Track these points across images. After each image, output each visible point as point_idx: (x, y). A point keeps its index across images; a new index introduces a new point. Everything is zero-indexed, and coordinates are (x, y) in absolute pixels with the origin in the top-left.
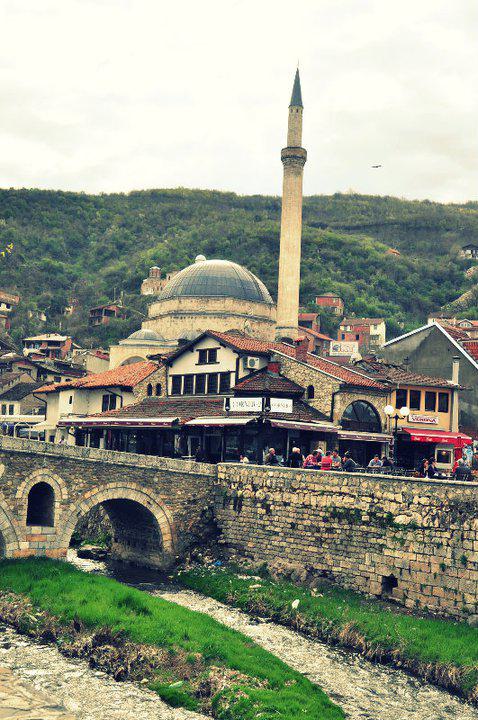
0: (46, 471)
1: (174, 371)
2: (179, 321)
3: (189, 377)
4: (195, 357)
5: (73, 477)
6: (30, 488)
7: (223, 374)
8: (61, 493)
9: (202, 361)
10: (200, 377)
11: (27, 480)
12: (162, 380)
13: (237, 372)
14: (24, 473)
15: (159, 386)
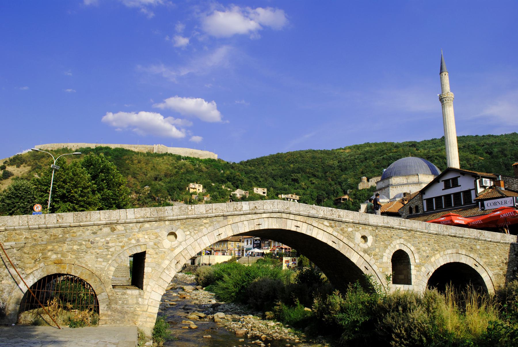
0: (402, 241)
1: (427, 196)
2: (394, 189)
3: (438, 199)
4: (442, 185)
5: (421, 245)
6: (392, 254)
7: (465, 192)
8: (414, 260)
9: (447, 187)
10: (447, 197)
11: (389, 247)
12: (418, 203)
13: (476, 189)
14: (386, 242)
15: (417, 207)
